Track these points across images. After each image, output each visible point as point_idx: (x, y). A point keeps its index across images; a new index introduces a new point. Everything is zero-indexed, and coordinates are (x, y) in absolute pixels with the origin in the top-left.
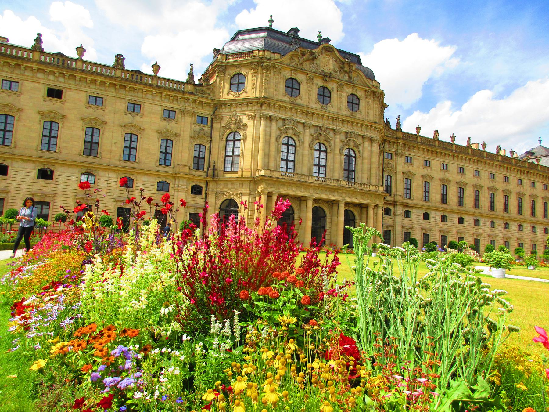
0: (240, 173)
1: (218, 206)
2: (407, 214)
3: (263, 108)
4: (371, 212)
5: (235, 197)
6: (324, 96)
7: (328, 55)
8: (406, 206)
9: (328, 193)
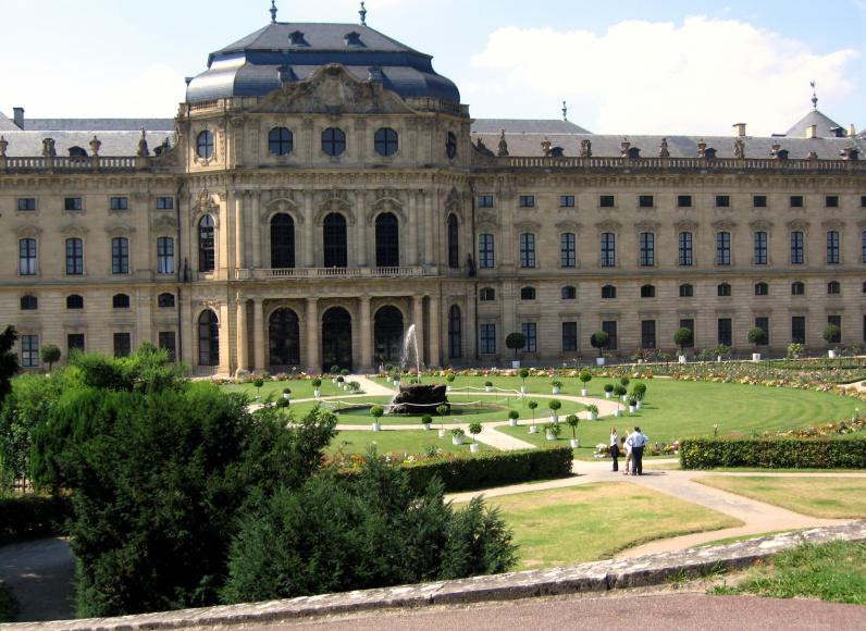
3: (237, 181)
4: (418, 308)
5: (212, 308)
6: (334, 142)
8: (521, 280)
9: (339, 289)
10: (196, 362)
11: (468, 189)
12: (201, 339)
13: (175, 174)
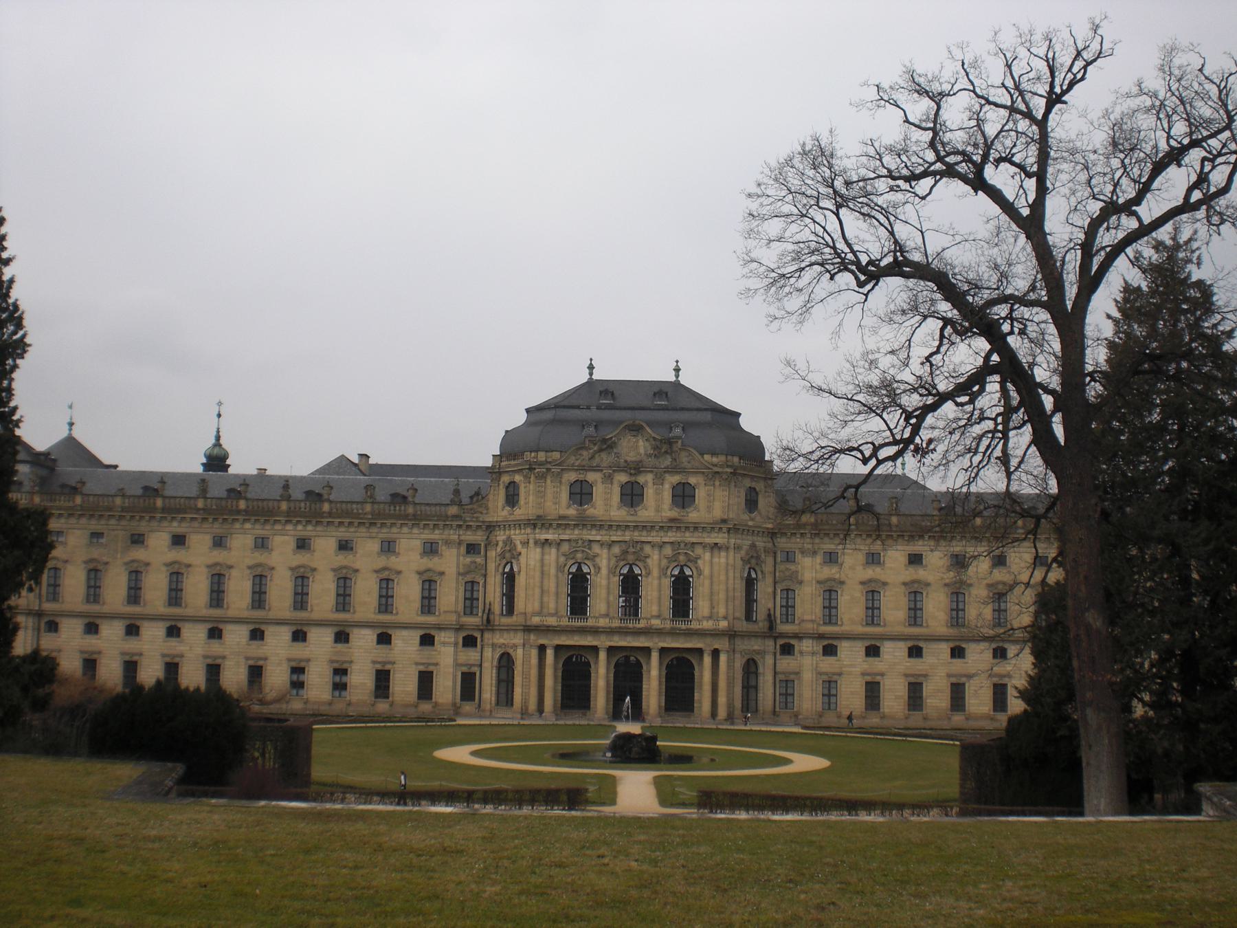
0: (514, 618)
1: (495, 663)
4: (707, 660)
6: (632, 495)
8: (821, 637)
9: (629, 638)
11: (770, 545)
12: (499, 681)
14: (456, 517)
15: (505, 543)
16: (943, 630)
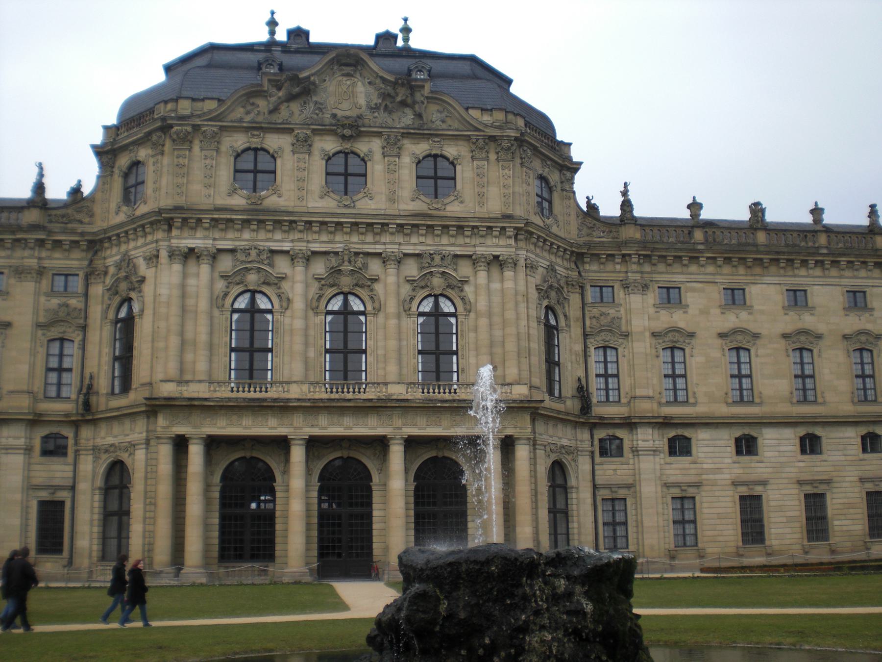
1: (99, 482)
2: (679, 447)
3: (175, 232)
6: (346, 175)
7: (348, 75)
8: (665, 423)
9: (347, 420)
10: (95, 554)
12: (107, 515)
13: (82, 234)
14: (34, 227)
15: (119, 267)
16: (847, 408)
